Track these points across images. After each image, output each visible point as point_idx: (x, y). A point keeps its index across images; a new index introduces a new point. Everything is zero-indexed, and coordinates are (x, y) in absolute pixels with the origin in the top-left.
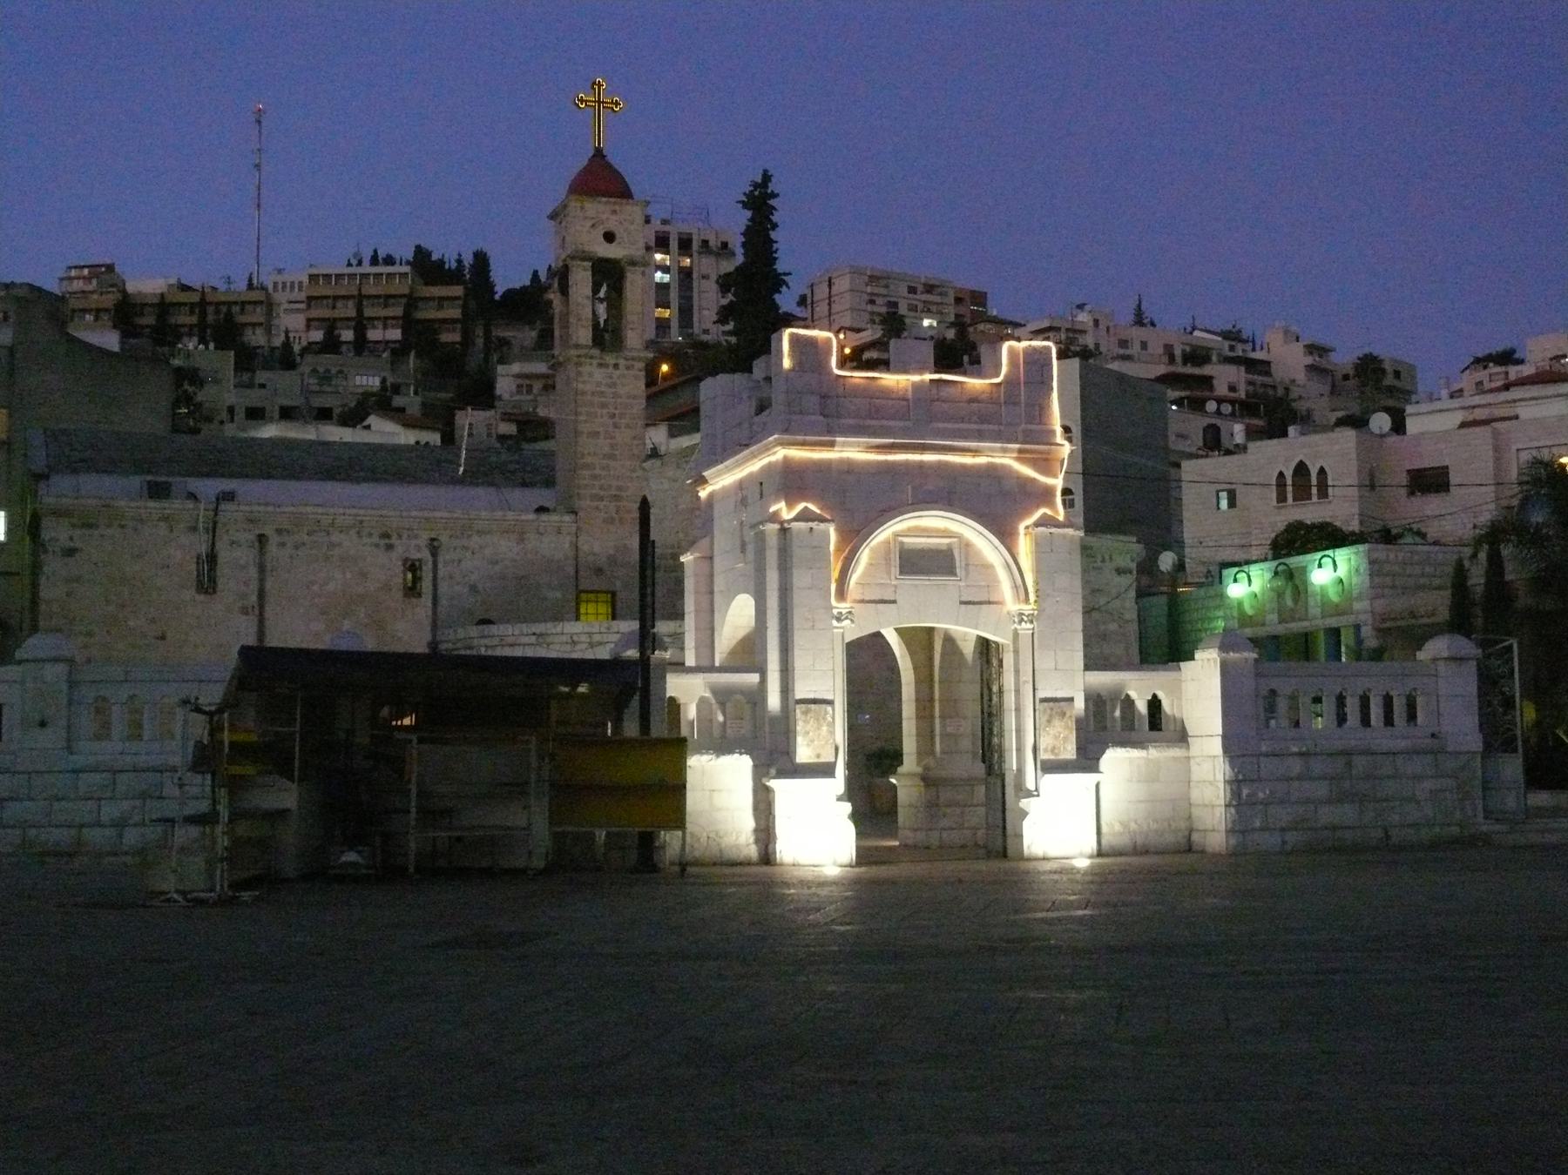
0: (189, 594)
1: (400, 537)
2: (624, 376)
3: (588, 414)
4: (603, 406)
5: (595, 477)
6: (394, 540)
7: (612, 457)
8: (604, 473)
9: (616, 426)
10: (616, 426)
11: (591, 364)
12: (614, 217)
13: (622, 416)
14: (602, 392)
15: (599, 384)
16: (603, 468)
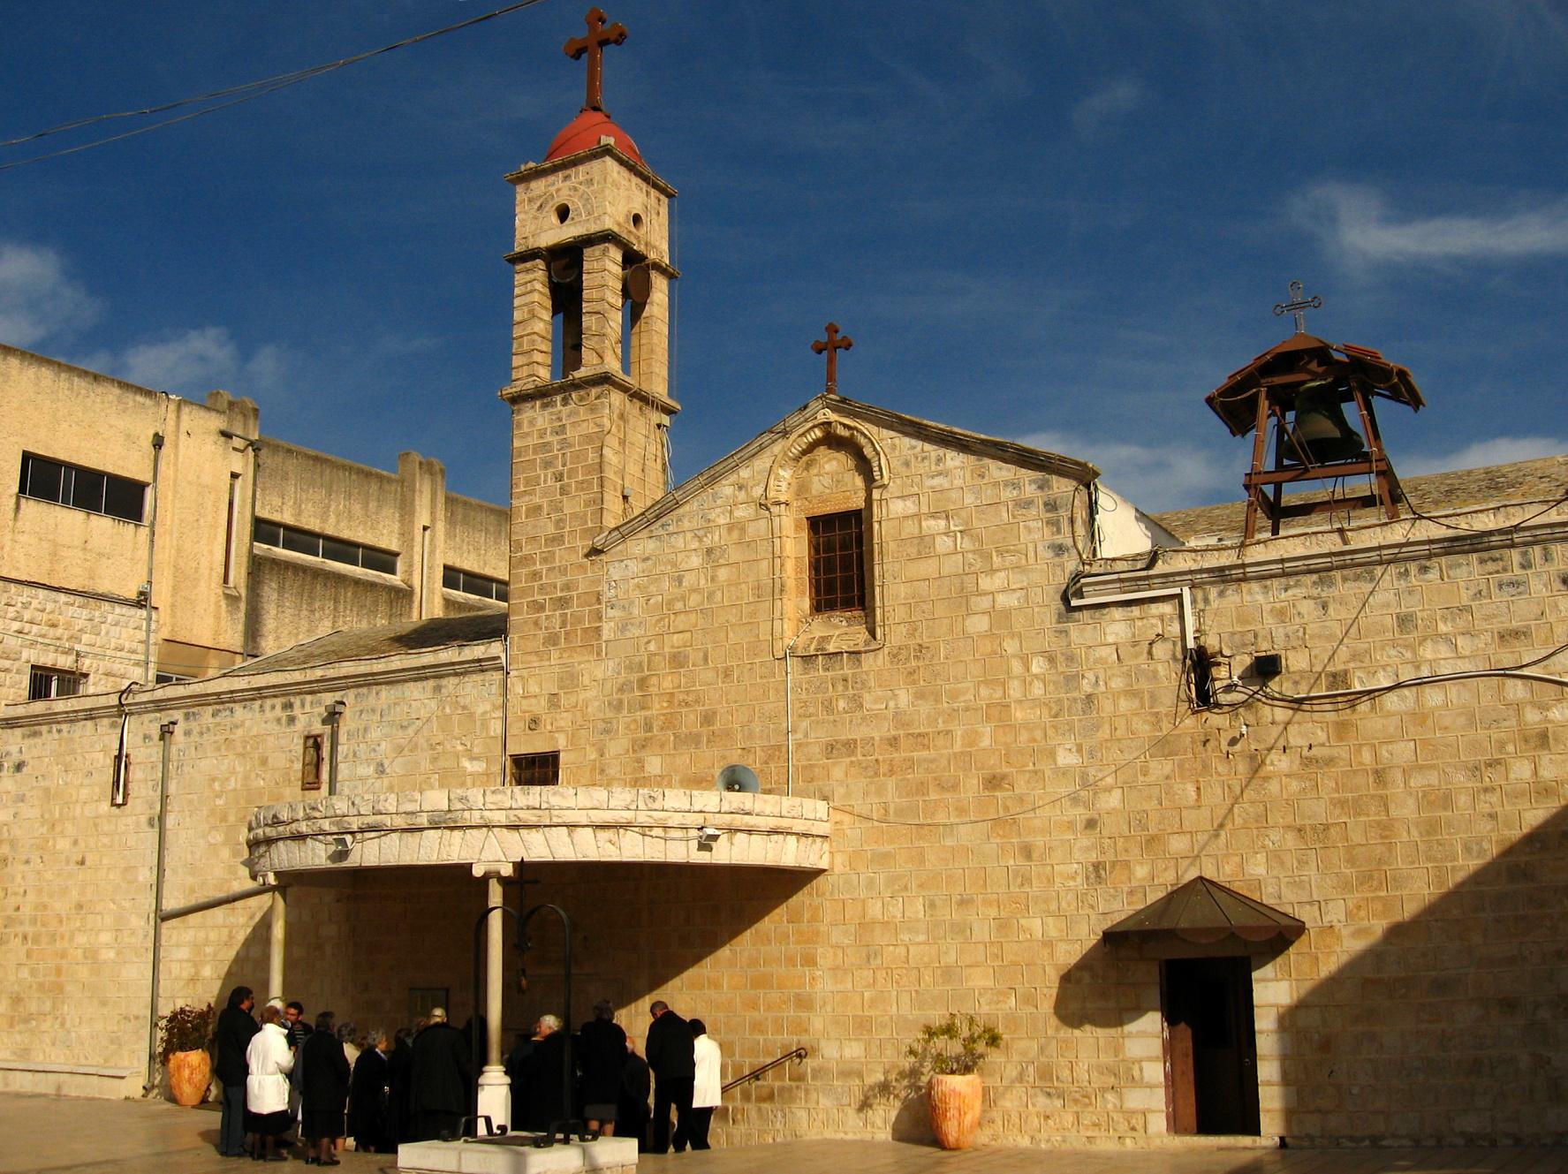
0: (105, 806)
1: (303, 705)
2: (577, 413)
3: (527, 483)
4: (547, 464)
5: (535, 575)
6: (297, 711)
7: (557, 539)
8: (545, 567)
9: (563, 491)
10: (564, 491)
11: (533, 407)
12: (568, 183)
13: (572, 472)
14: (544, 445)
15: (542, 434)
16: (545, 560)
